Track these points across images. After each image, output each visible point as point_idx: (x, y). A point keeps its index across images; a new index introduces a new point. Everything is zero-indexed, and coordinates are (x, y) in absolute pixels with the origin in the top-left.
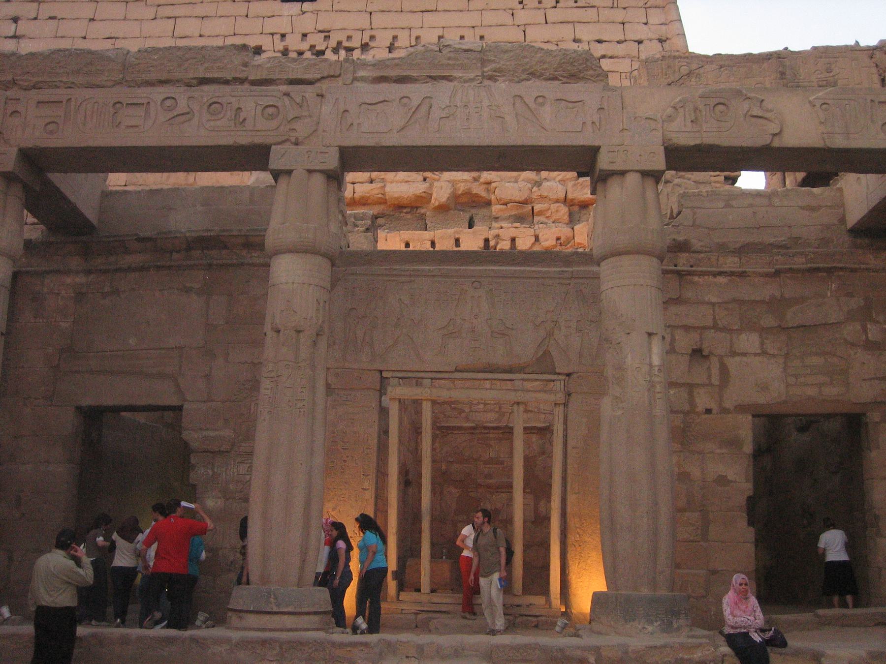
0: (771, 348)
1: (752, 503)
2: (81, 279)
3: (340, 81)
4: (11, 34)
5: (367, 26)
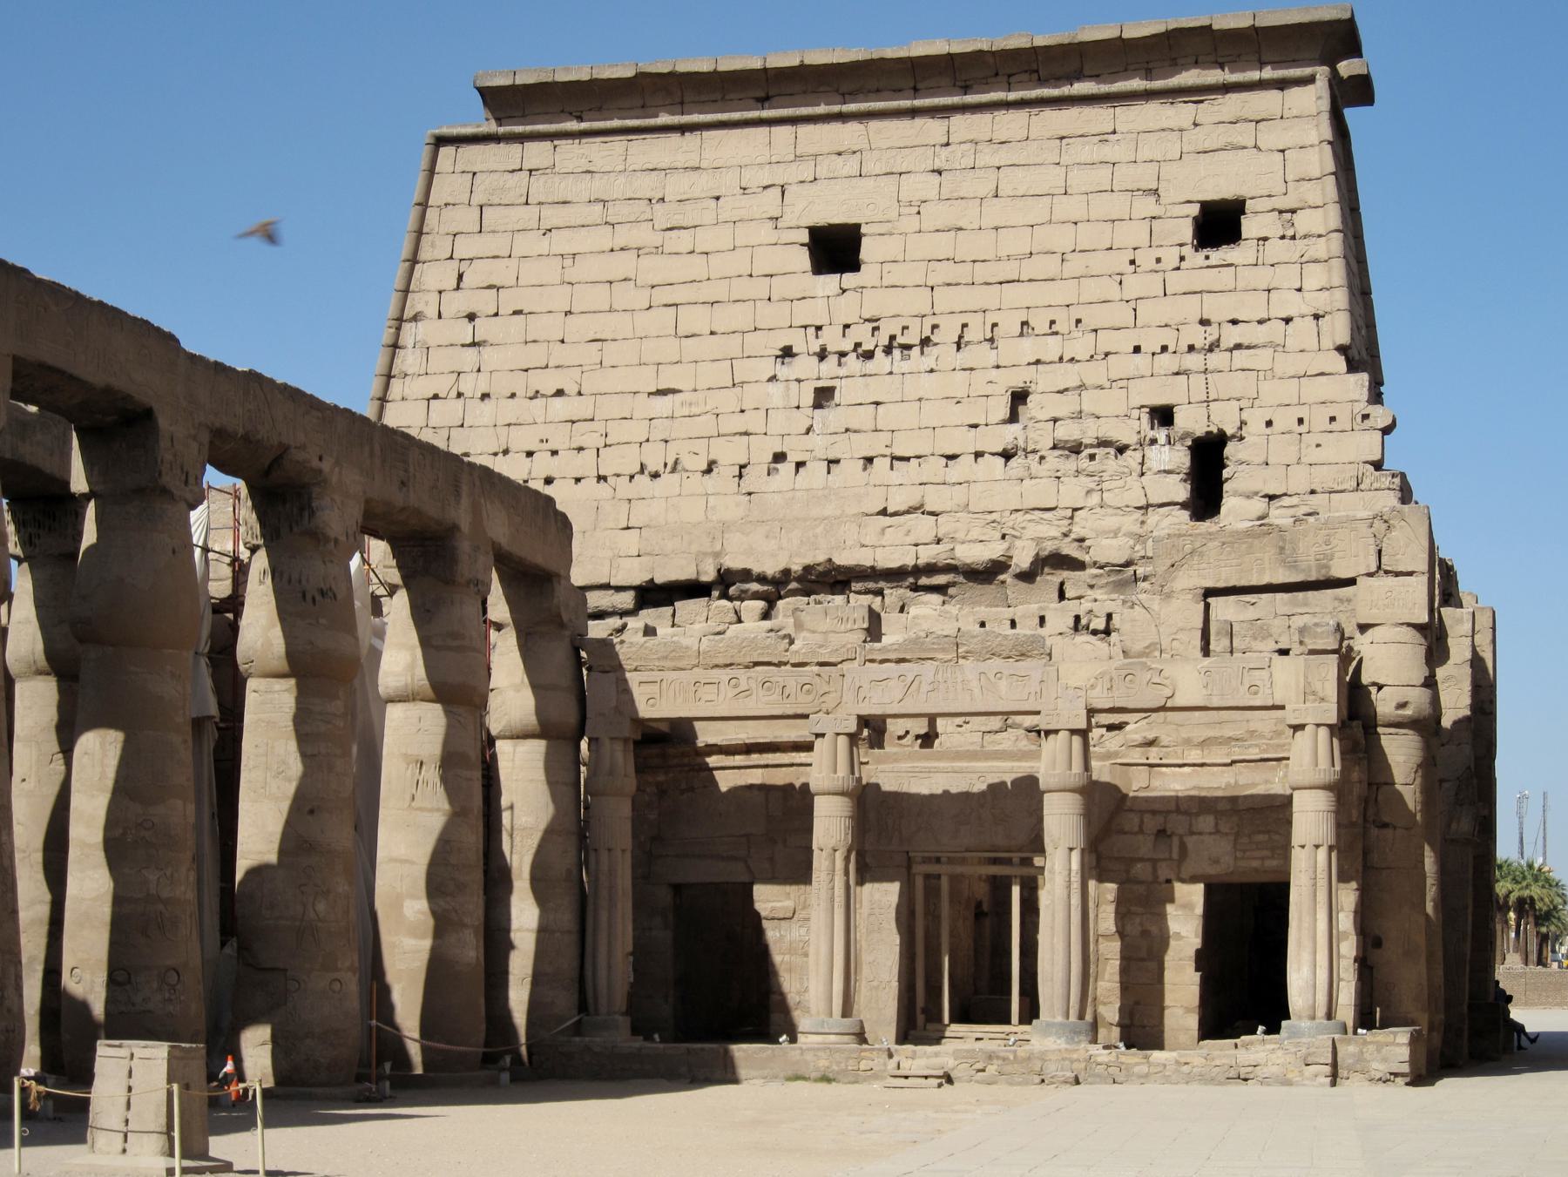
0: (1224, 828)
1: (1200, 955)
2: (661, 778)
3: (856, 663)
4: (469, 340)
5: (928, 310)
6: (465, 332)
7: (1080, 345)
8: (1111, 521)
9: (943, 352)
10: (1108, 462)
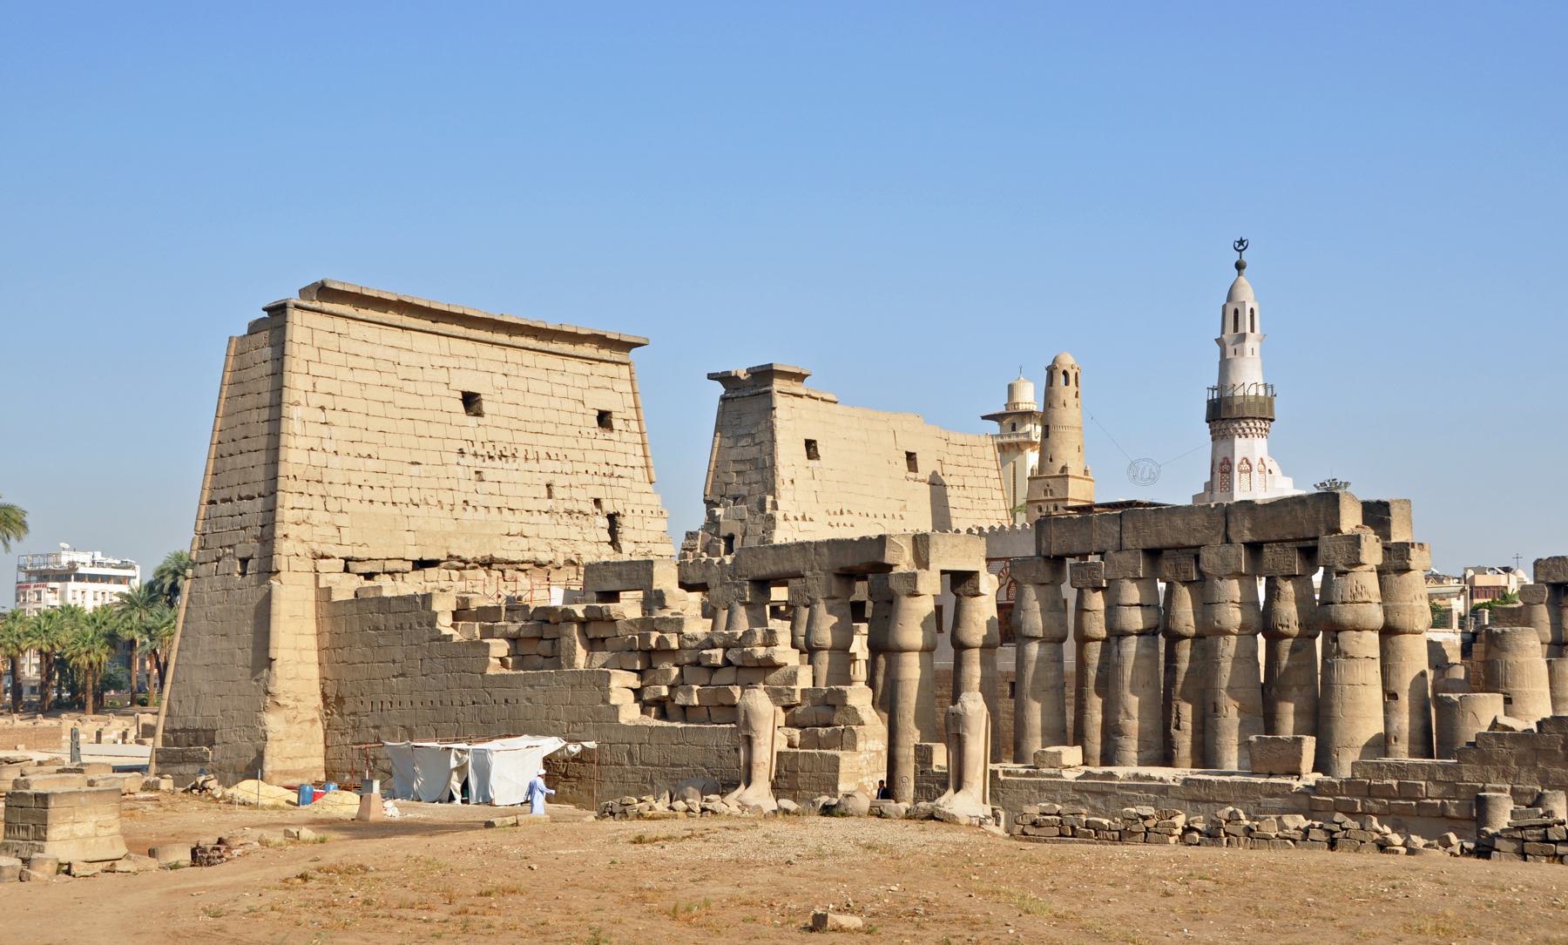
6: (321, 417)
7: (568, 467)
8: (588, 547)
9: (520, 460)
10: (582, 521)
